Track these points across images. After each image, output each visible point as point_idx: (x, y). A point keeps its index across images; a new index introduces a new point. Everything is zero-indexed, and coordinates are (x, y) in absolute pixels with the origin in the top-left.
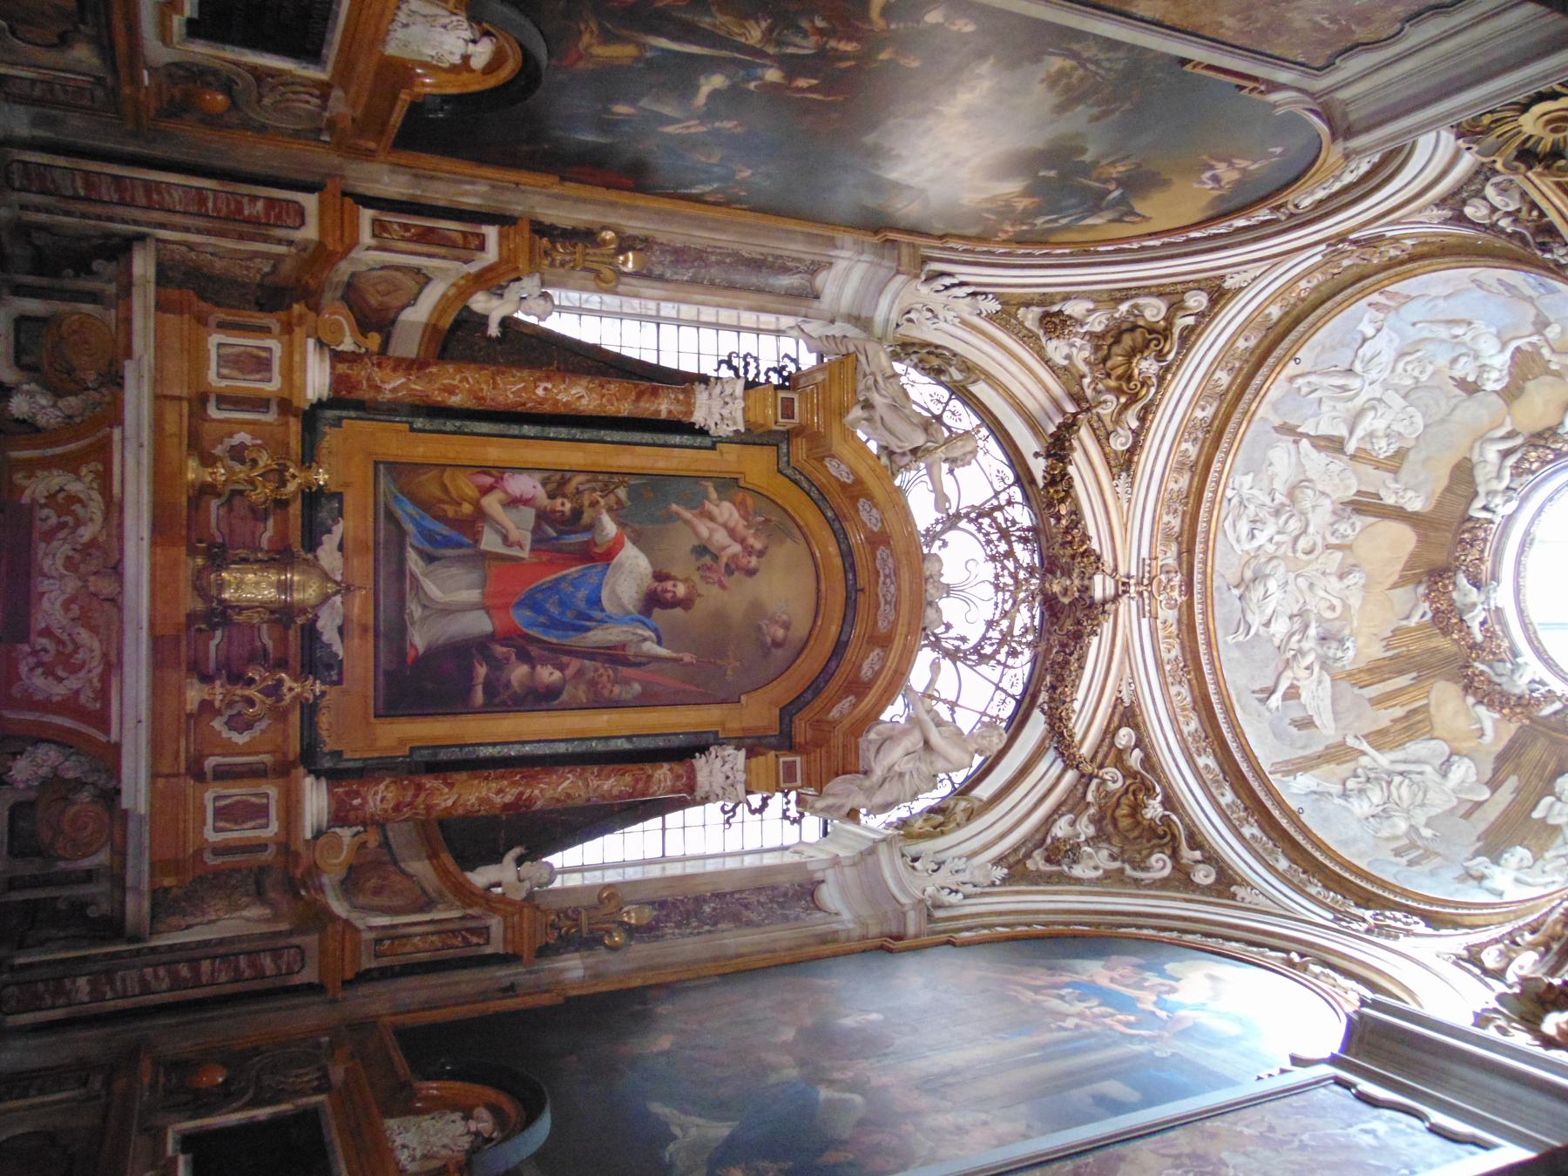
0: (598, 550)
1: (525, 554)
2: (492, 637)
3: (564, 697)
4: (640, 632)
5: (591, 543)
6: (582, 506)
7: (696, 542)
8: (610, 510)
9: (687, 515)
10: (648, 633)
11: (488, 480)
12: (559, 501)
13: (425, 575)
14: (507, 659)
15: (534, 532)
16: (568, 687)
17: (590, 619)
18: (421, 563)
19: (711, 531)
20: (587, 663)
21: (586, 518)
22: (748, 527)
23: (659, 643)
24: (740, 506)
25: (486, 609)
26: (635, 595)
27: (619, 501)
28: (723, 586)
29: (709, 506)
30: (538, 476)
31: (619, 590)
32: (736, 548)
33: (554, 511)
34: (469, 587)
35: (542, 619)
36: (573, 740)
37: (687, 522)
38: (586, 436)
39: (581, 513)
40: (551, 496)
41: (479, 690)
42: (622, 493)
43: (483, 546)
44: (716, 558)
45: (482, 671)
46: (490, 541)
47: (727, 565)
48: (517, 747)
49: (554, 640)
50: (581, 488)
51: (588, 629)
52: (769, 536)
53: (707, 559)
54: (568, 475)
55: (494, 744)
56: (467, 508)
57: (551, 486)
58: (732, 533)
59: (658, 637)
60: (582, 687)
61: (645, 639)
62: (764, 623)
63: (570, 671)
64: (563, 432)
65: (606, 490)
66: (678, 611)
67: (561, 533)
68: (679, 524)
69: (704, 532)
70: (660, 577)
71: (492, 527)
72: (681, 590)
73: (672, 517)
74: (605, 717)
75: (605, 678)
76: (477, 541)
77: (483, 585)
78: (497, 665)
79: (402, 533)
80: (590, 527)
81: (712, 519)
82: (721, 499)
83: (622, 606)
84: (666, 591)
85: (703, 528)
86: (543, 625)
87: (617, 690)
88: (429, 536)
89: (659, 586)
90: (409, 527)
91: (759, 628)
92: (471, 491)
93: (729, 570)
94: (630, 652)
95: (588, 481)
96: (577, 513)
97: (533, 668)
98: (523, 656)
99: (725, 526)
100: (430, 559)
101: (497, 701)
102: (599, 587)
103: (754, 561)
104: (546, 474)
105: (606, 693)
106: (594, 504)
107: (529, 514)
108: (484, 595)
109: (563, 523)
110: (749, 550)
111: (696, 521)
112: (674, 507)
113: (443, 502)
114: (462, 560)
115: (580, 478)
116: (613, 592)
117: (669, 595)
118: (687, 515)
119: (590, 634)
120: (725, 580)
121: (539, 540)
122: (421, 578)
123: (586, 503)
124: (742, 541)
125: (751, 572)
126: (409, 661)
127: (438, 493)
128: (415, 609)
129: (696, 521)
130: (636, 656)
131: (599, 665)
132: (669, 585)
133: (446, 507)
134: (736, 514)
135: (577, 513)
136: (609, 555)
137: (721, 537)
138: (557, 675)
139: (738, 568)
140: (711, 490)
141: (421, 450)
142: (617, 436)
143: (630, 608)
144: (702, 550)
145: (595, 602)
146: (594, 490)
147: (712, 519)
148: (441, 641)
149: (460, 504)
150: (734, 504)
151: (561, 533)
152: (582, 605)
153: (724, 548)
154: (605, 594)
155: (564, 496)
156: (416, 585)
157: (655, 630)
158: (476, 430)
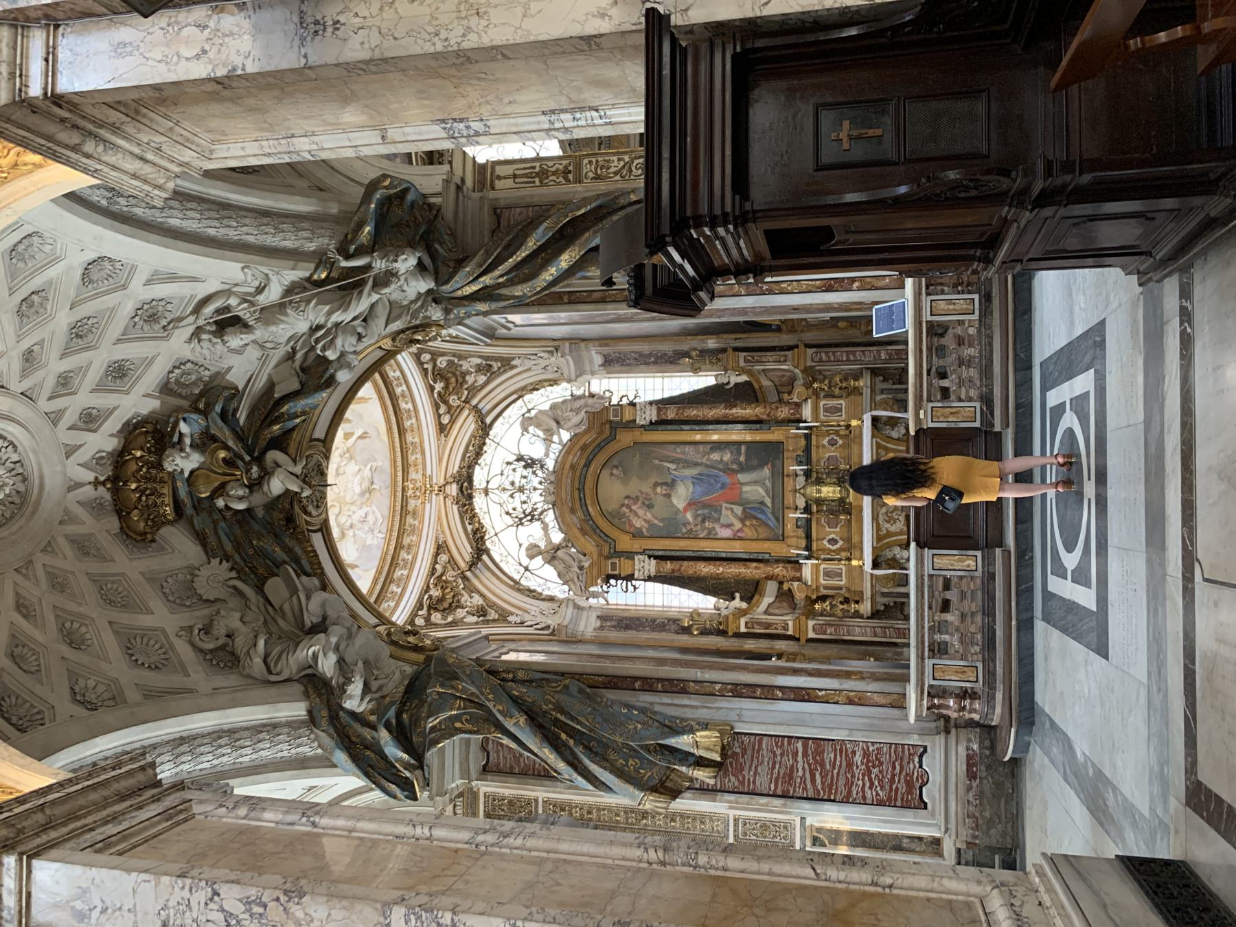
1: (724, 505)
9: (656, 521)
24: (632, 525)
28: (641, 492)
29: (646, 525)
30: (719, 536)
32: (634, 508)
40: (714, 528)
43: (741, 508)
44: (643, 503)
45: (742, 459)
46: (738, 510)
51: (699, 474)
53: (647, 503)
56: (748, 523)
58: (636, 514)
70: (668, 496)
72: (659, 490)
73: (662, 520)
76: (744, 510)
77: (741, 492)
79: (773, 513)
82: (641, 529)
85: (649, 516)
88: (763, 512)
90: (770, 516)
93: (638, 497)
96: (703, 521)
99: (639, 517)
100: (762, 503)
107: (723, 521)
108: (741, 489)
110: (628, 507)
114: (749, 503)
116: (688, 490)
118: (656, 521)
124: (631, 510)
125: (628, 497)
127: (759, 529)
132: (664, 492)
137: (641, 512)
156: (767, 491)
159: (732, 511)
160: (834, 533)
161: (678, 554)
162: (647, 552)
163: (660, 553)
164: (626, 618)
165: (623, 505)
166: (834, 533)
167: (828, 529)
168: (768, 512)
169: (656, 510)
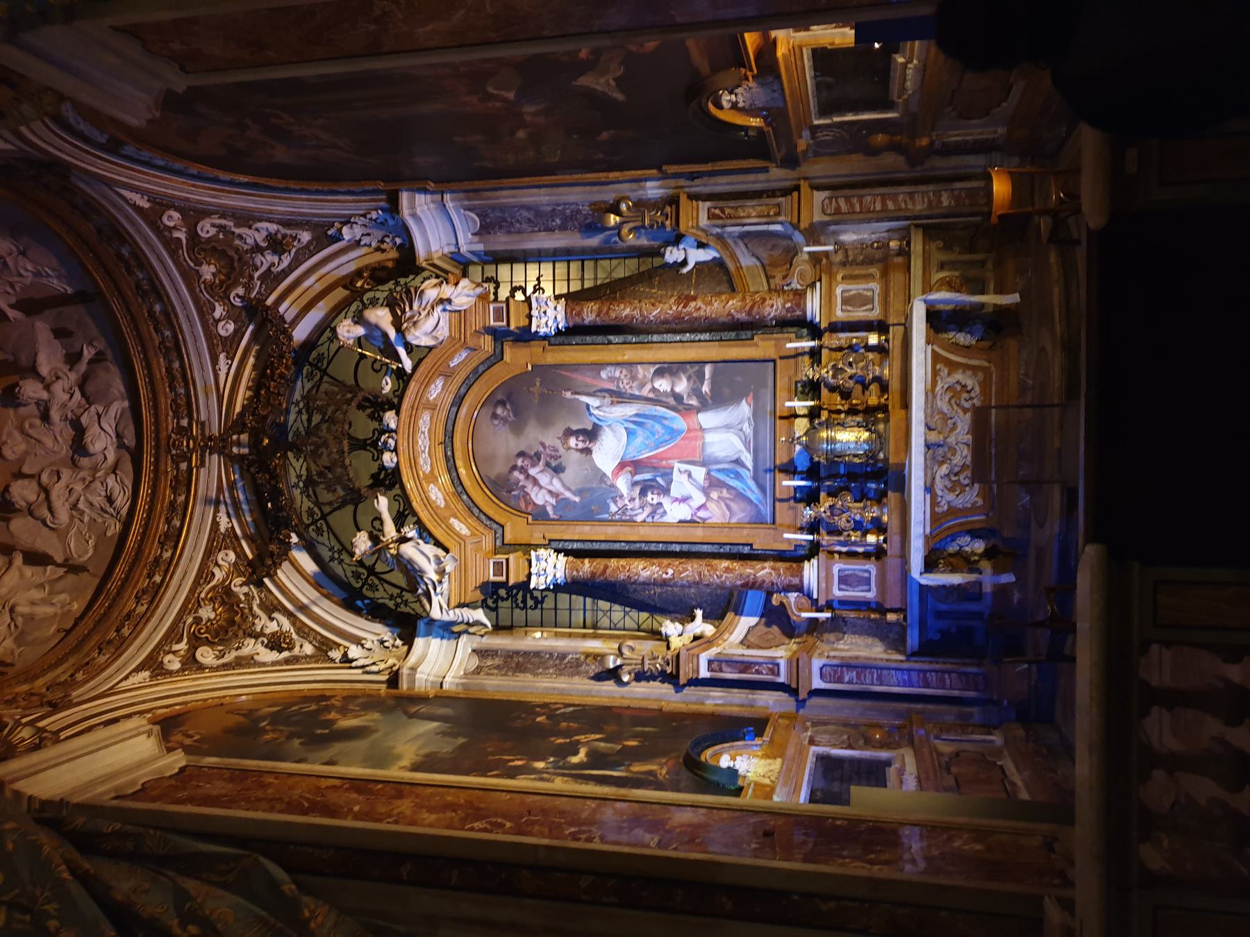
0: (629, 468)
1: (677, 466)
2: (699, 411)
3: (652, 370)
4: (601, 413)
5: (634, 474)
7: (562, 475)
8: (621, 496)
10: (596, 412)
12: (655, 502)
17: (634, 422)
18: (743, 459)
19: (551, 483)
20: (637, 393)
21: (637, 490)
22: (524, 487)
23: (588, 406)
24: (529, 501)
25: (702, 429)
26: (603, 437)
27: (615, 502)
28: (543, 445)
29: (553, 501)
32: (532, 472)
34: (713, 443)
37: (568, 489)
38: (638, 545)
40: (660, 504)
41: (707, 376)
42: (613, 508)
43: (703, 470)
44: (548, 465)
45: (706, 388)
49: (658, 408)
50: (641, 510)
51: (637, 415)
52: (509, 480)
53: (554, 463)
56: (714, 495)
57: (660, 511)
58: (535, 482)
59: (588, 409)
60: (640, 376)
61: (597, 408)
62: (512, 418)
63: (649, 387)
64: (653, 547)
65: (624, 509)
66: (575, 427)
67: (654, 480)
68: (573, 488)
70: (587, 451)
71: (698, 483)
72: (572, 442)
73: (579, 492)
75: (625, 382)
76: (708, 473)
78: (696, 392)
80: (635, 484)
81: (550, 492)
82: (544, 507)
83: (613, 430)
85: (557, 486)
86: (666, 419)
87: (617, 374)
88: (738, 476)
91: (515, 415)
92: (711, 505)
93: (538, 456)
94: (608, 400)
96: (643, 493)
98: (678, 398)
99: (541, 487)
100: (738, 462)
102: (628, 444)
103: (519, 462)
105: (624, 372)
106: (632, 500)
108: (703, 438)
109: (652, 487)
110: (523, 470)
112: (577, 499)
113: (730, 499)
114: (718, 462)
117: (581, 438)
118: (568, 494)
119: (634, 412)
121: (668, 475)
123: (637, 500)
124: (528, 476)
125: (522, 454)
128: (748, 429)
130: (604, 397)
131: (629, 391)
132: (581, 445)
133: (728, 496)
134: (533, 496)
135: (643, 493)
136: (622, 465)
137: (544, 479)
138: (657, 385)
139: (531, 458)
142: (617, 546)
143: (607, 429)
144: (558, 470)
145: (630, 433)
147: (550, 492)
149: (719, 497)
150: (534, 504)
151: (654, 480)
152: (640, 431)
153: (542, 471)
155: (652, 505)
156: (746, 443)
157: (591, 414)
159: (690, 475)
161: (604, 546)
162: (554, 545)
163: (575, 546)
164: (517, 653)
165: (514, 468)
168: (747, 475)
169: (570, 475)
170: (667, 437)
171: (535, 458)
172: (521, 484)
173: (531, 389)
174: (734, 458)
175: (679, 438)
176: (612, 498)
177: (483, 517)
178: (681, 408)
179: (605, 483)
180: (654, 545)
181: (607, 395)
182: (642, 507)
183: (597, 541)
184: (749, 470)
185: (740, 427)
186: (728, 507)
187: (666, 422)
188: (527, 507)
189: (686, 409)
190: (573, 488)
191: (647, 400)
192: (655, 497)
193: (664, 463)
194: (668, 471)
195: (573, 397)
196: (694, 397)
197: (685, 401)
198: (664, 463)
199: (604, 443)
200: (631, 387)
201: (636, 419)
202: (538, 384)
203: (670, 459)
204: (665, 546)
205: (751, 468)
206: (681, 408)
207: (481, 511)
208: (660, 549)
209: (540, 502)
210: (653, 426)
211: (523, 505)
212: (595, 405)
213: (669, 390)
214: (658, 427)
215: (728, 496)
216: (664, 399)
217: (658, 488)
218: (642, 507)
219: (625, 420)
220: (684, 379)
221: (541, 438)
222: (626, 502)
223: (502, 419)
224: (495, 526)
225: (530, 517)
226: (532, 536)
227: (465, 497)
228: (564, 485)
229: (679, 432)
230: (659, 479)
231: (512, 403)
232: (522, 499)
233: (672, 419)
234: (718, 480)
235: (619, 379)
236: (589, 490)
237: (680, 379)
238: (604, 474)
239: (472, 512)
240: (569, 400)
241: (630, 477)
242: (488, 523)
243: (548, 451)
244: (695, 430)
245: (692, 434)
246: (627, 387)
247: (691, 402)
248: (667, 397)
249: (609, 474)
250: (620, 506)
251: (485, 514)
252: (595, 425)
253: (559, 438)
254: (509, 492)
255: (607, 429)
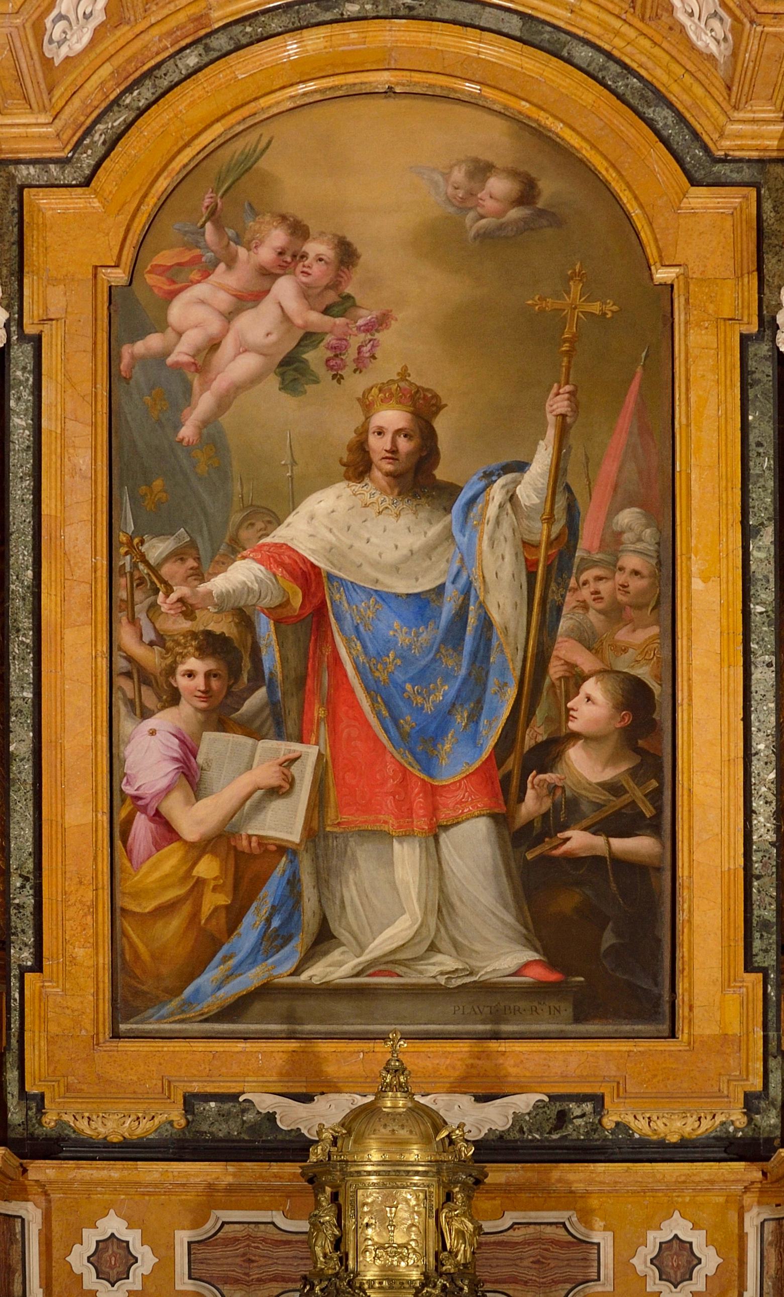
0: (297, 601)
1: (310, 752)
2: (501, 820)
3: (643, 672)
4: (492, 510)
6: (194, 635)
7: (273, 382)
8: (199, 575)
9: (204, 403)
10: (497, 493)
11: (142, 827)
12: (182, 682)
13: (362, 948)
14: (553, 789)
15: (256, 735)
16: (623, 664)
17: (461, 615)
18: (336, 955)
19: (244, 349)
20: (564, 624)
21: (223, 626)
22: (231, 262)
23: (521, 467)
26: (407, 519)
27: (178, 555)
28: (381, 322)
29: (181, 354)
30: (126, 725)
31: (391, 556)
33: (207, 693)
34: (390, 863)
35: (461, 718)
36: (747, 652)
37: (223, 404)
38: (26, 623)
39: (208, 634)
40: (174, 698)
41: (620, 844)
43: (294, 835)
44: (309, 338)
47: (326, 311)
48: (756, 765)
49: (511, 693)
51: (486, 624)
53: (314, 357)
54: (121, 664)
55: (749, 813)
56: (207, 868)
57: (149, 698)
59: (507, 469)
60: (623, 635)
61: (512, 498)
62: (473, 225)
63: (585, 661)
66: (441, 424)
67: (258, 678)
68: (225, 420)
69: (248, 364)
71: (249, 818)
74: (697, 584)
75: (604, 588)
76: (282, 849)
79: (266, 991)
81: (214, 345)
82: (162, 325)
83: (429, 551)
84: (394, 451)
86: (474, 718)
87: (631, 561)
89: (382, 466)
90: (253, 978)
91: (485, 236)
94: (540, 532)
95: (133, 621)
97: (575, 736)
99: (229, 316)
101: (648, 811)
102: (384, 597)
103: (316, 248)
104: (121, 708)
105: (636, 584)
106: (187, 609)
108: (406, 835)
109: (234, 673)
111: (220, 383)
112: (187, 432)
113: (195, 915)
114: (322, 881)
115: (126, 637)
116: (395, 569)
117: (404, 445)
118: (204, 403)
119: (496, 616)
120: (365, 317)
122: (366, 957)
123: (186, 625)
124: (269, 275)
126: (553, 977)
127: (176, 923)
129: (220, 383)
130: (550, 520)
131: (570, 600)
132: (378, 445)
133: (206, 910)
134: (200, 290)
138: (590, 687)
139: (335, 285)
140: (140, 347)
141: (80, 953)
143: (435, 530)
146: (153, 607)
147: (214, 345)
148: (510, 919)
149: (200, 882)
150: (172, 295)
152: (428, 635)
153: (286, 317)
154: (402, 587)
155: (171, 671)
157: (489, 477)
158: (29, 847)
159: (274, 792)
160: (165, 1263)
166: (165, 1263)
167: (183, 1237)
170: (408, 721)
171: (331, 297)
172: (242, 252)
173: (576, 288)
174: (336, 927)
175: (407, 760)
176: (192, 544)
177: (118, 120)
178: (512, 763)
179: (248, 521)
180: (29, 671)
181: (556, 529)
182: (160, 640)
183: (37, 491)
184: (296, 972)
185: (445, 944)
186: (165, 910)
187: (461, 718)
188: (162, 270)
189: (506, 781)
190: (225, 420)
191: (542, 659)
192: (199, 682)
193: (319, 712)
194: (291, 726)
195: (551, 418)
196: (547, 804)
197: (533, 778)
198: (319, 712)
199: (388, 520)
200: (585, 606)
201: (472, 620)
202: (595, 308)
203: (333, 732)
204: (27, 708)
205: (304, 977)
206: (512, 763)
207: (142, 112)
208: (14, 691)
209: (177, 312)
210: (447, 677)
211: (166, 258)
212: (520, 491)
213: (573, 726)
214: (443, 692)
215: (206, 910)
216: (540, 713)
217: (229, 693)
218: (160, 640)
219: (469, 584)
220: (608, 775)
221: (402, 317)
222: (180, 591)
223: (471, 194)
224: (87, 160)
225: (119, 276)
226: (54, 281)
227: (192, 60)
228: (237, 389)
229: (427, 763)
230: (261, 694)
231: (526, 227)
232: (186, 257)
233: (474, 738)
234: (260, 881)
235: (614, 566)
236: (223, 473)
237: (612, 760)
238: (278, 521)
239: (138, 82)
240: (540, 407)
241: (266, 602)
242: (98, 138)
243: (355, 342)
244: (434, 810)
245: (419, 801)
246: (585, 593)
247: (530, 793)
248: (548, 720)
249: (280, 535)
250: (165, 571)
251: (129, 126)
252: (452, 491)
253: (404, 374)
254: (213, 214)
255: (435, 530)
